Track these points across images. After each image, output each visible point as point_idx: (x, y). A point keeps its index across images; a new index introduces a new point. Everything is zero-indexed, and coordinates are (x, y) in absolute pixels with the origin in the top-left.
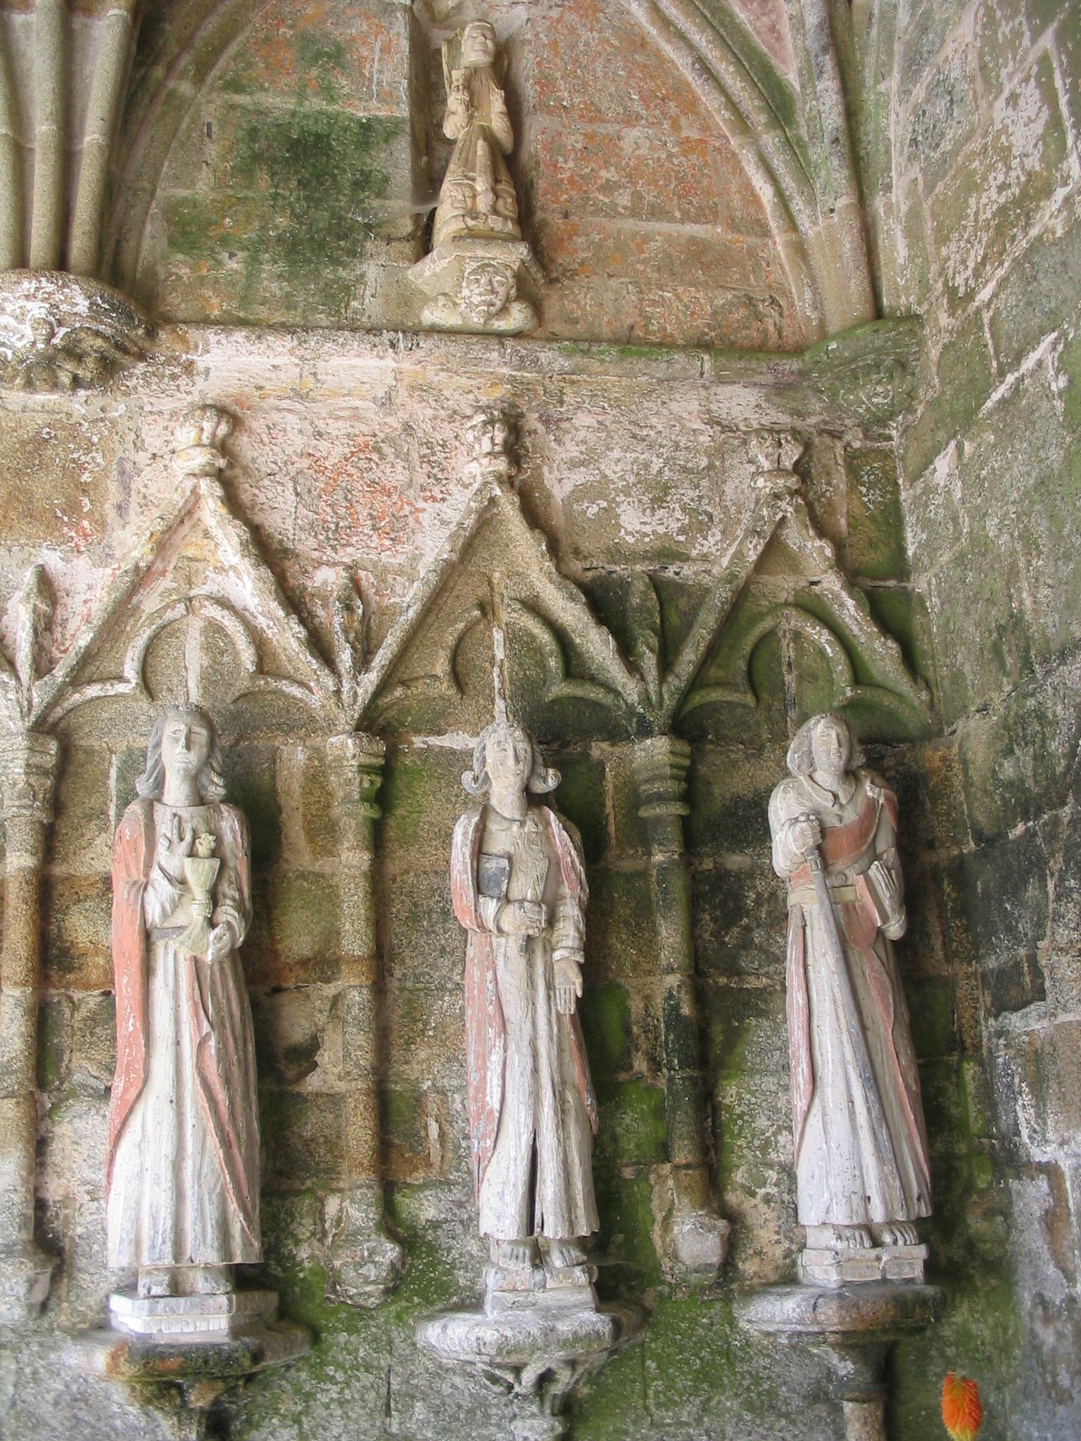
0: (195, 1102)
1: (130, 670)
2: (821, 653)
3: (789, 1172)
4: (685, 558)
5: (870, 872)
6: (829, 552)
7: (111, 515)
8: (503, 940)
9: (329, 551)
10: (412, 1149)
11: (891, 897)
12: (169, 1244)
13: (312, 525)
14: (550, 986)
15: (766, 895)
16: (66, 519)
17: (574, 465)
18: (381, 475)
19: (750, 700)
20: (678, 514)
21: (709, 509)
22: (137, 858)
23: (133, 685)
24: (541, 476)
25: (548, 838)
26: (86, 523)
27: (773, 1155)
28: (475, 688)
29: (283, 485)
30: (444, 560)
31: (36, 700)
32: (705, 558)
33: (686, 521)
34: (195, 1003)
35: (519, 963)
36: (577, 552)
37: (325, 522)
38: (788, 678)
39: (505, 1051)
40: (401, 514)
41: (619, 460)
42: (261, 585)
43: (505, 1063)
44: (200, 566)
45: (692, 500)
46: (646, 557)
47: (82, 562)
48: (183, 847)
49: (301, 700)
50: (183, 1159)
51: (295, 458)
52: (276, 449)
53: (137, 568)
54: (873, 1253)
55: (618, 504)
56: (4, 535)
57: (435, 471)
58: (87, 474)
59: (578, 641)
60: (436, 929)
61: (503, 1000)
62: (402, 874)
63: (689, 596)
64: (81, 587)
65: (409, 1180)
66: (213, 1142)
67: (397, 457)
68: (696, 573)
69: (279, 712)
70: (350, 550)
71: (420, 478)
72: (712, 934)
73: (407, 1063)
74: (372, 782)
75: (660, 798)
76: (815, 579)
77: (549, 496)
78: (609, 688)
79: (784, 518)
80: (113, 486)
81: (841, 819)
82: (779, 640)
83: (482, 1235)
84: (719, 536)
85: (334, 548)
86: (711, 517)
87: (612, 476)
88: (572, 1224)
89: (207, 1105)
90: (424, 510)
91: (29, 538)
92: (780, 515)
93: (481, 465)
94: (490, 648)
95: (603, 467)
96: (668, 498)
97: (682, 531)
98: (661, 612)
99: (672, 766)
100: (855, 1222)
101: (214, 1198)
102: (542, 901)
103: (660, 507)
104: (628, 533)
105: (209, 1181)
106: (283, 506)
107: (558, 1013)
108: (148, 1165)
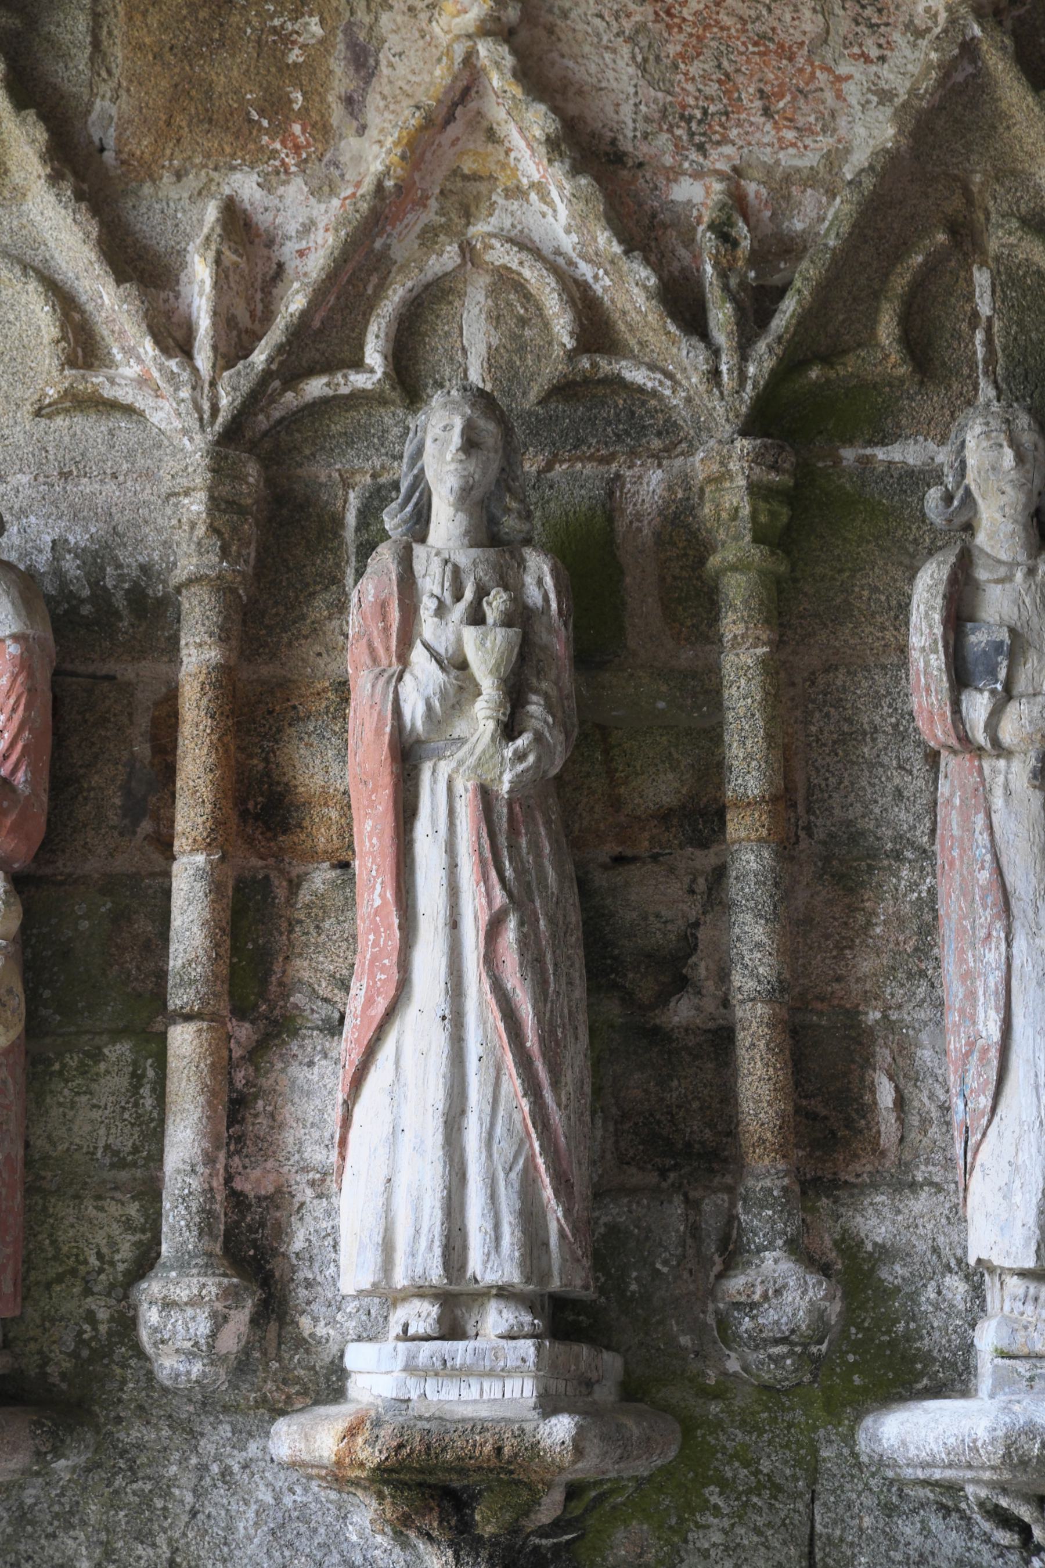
0: (483, 1021)
1: (374, 356)
7: (337, 114)
8: (1002, 763)
9: (694, 155)
10: (849, 1123)
12: (438, 1251)
13: (664, 112)
16: (265, 123)
18: (776, 24)
22: (386, 630)
23: (379, 374)
26: (297, 128)
28: (944, 364)
29: (614, 51)
30: (887, 151)
31: (224, 402)
34: (482, 862)
37: (684, 107)
39: (1009, 945)
40: (812, 87)
42: (581, 206)
44: (483, 187)
47: (295, 190)
48: (459, 610)
49: (654, 393)
50: (463, 1112)
53: (379, 187)
56: (168, 152)
58: (297, 51)
60: (885, 760)
61: (1004, 860)
62: (827, 671)
64: (292, 228)
65: (844, 1176)
66: (512, 1084)
69: (617, 415)
70: (728, 150)
71: (843, 26)
73: (839, 979)
74: (773, 514)
80: (338, 66)
83: (972, 1261)
85: (701, 148)
89: (501, 1026)
90: (850, 77)
91: (208, 155)
94: (970, 297)
101: (513, 1175)
105: (504, 1148)
106: (614, 85)
108: (406, 1122)
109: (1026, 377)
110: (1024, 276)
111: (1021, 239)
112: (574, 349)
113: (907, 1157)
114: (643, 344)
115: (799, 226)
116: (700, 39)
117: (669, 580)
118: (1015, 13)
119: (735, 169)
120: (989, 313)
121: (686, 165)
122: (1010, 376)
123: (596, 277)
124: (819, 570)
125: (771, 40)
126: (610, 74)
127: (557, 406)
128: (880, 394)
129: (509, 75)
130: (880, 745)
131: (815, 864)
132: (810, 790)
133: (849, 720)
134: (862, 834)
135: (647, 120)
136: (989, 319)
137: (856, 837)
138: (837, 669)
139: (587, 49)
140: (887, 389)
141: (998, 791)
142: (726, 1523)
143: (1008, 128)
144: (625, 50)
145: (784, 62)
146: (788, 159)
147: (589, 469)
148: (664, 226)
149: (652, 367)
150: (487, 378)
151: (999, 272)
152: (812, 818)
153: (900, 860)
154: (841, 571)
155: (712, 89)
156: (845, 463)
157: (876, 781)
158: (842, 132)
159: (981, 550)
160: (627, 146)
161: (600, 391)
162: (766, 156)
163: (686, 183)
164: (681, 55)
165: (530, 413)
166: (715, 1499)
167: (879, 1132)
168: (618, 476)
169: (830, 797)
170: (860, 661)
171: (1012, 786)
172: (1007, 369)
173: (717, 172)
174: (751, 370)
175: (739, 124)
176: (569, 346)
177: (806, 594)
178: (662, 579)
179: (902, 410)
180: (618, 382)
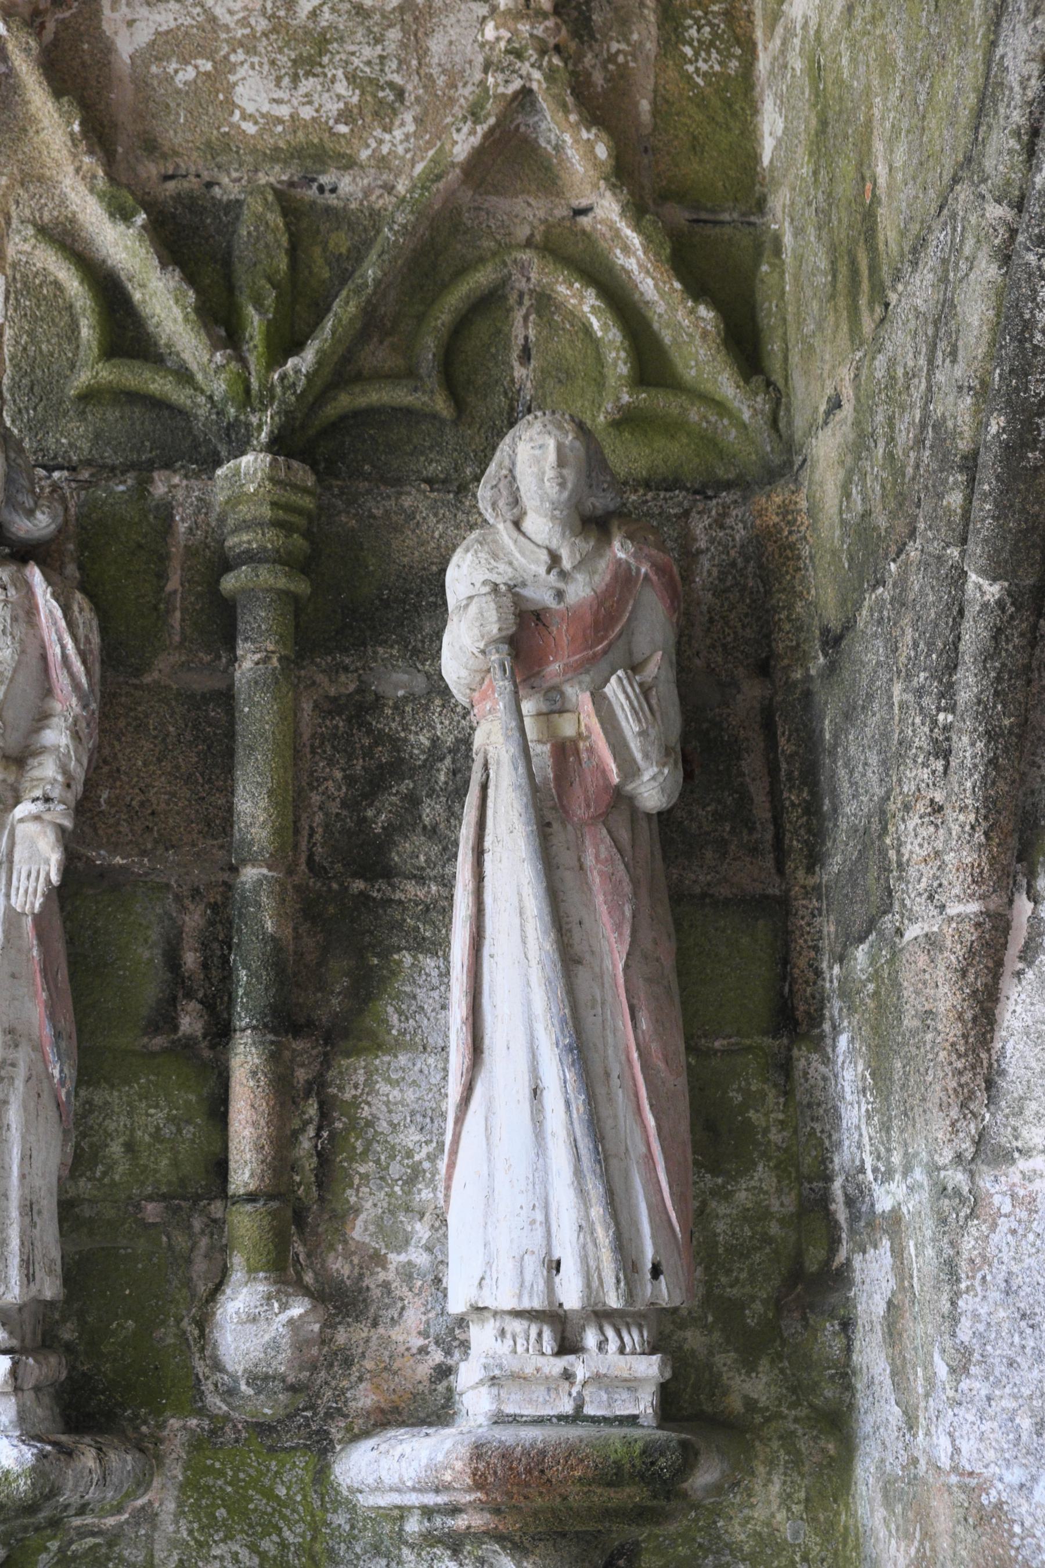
2: (587, 330)
3: (441, 1221)
4: (349, 163)
5: (608, 690)
6: (602, 151)
11: (643, 733)
15: (450, 740)
19: (441, 405)
20: (341, 87)
21: (397, 79)
32: (382, 162)
33: (355, 100)
36: (151, 146)
38: (519, 372)
45: (369, 63)
46: (275, 156)
54: (557, 1365)
55: (233, 69)
59: (137, 296)
63: (351, 228)
68: (367, 192)
72: (344, 804)
75: (250, 557)
76: (584, 203)
77: (108, 49)
78: (184, 376)
79: (526, 93)
81: (560, 595)
82: (510, 310)
84: (411, 128)
86: (400, 93)
87: (225, 18)
92: (517, 84)
96: (325, 60)
97: (346, 116)
98: (293, 251)
99: (274, 505)
100: (526, 1305)
103: (307, 74)
104: (244, 117)
109: (32, 389)
110: (41, 286)
111: (34, 247)
118: (60, 16)
143: (37, 132)
151: (14, 278)
172: (13, 379)
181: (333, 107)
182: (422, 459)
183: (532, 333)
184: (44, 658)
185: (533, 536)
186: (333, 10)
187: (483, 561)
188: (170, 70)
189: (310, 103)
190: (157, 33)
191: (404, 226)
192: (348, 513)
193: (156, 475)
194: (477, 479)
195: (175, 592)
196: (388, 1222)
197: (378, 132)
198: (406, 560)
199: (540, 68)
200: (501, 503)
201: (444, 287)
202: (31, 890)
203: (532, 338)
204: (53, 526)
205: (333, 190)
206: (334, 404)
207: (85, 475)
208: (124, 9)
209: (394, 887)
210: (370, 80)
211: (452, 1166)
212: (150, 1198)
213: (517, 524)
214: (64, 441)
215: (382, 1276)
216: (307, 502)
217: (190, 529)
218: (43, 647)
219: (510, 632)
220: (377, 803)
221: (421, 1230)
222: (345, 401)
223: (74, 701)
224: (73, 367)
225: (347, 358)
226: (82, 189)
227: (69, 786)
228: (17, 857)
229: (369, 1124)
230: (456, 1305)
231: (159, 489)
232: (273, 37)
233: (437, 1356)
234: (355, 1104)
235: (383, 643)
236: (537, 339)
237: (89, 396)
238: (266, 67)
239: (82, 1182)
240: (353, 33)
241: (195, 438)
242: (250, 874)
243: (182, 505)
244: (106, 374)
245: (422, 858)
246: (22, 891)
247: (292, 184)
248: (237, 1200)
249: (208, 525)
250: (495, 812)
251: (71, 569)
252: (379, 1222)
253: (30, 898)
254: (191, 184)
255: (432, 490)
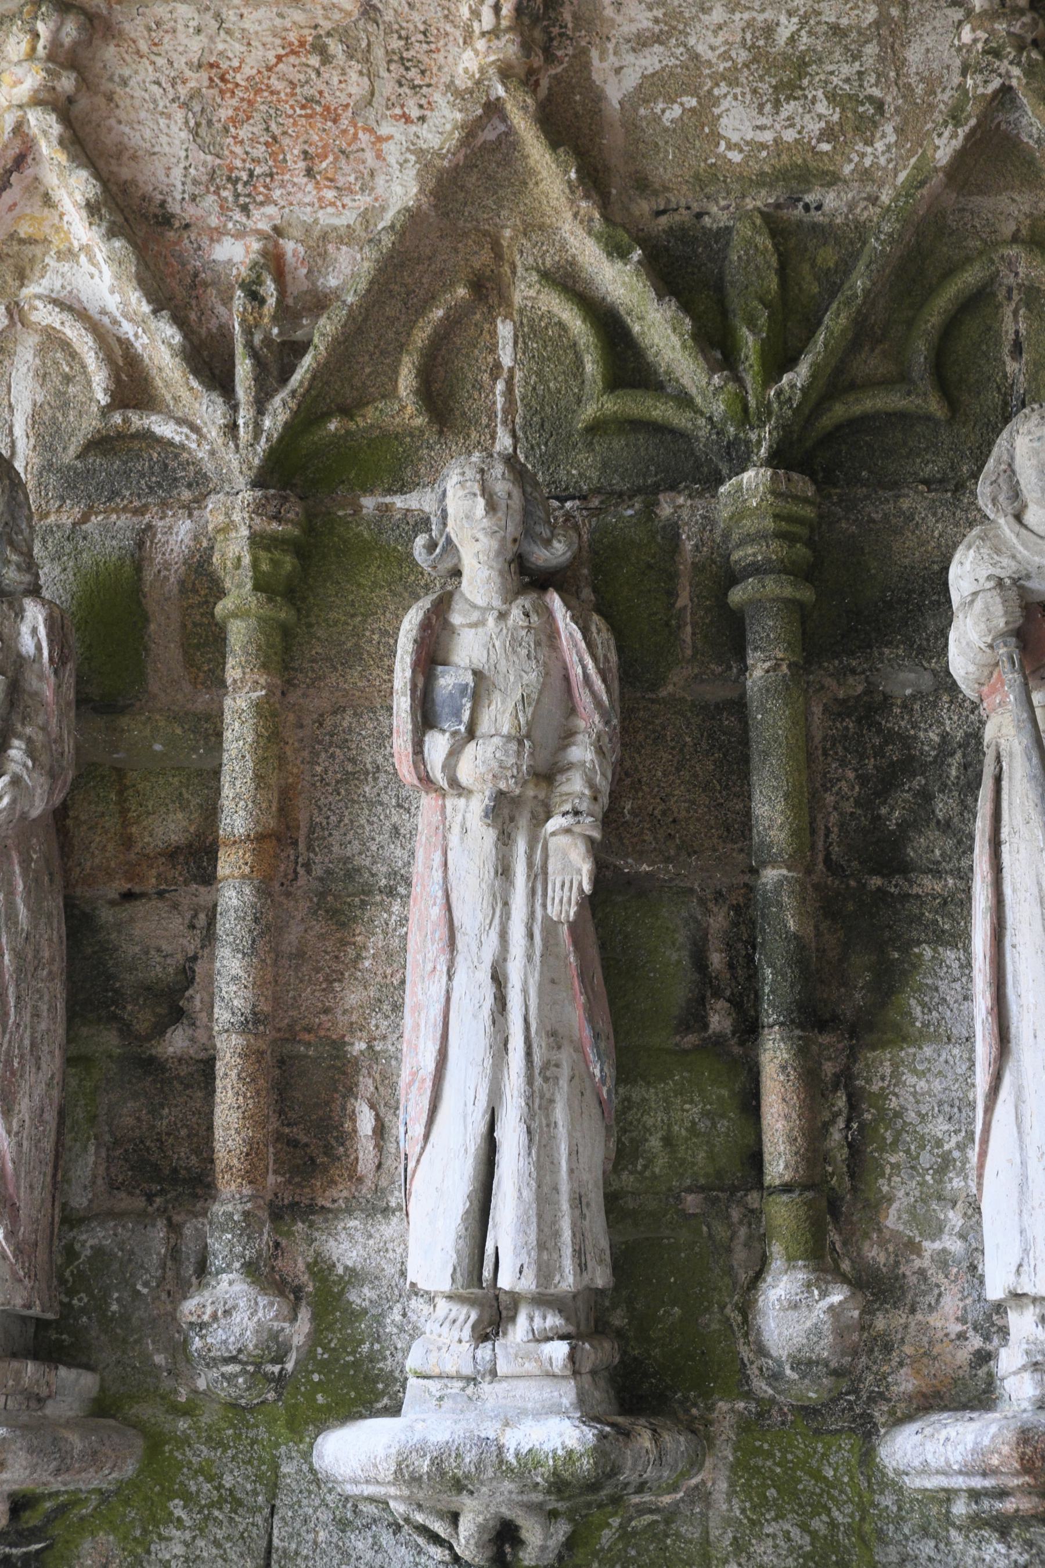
8: (462, 801)
9: (238, 216)
10: (328, 1150)
13: (212, 175)
14: (538, 876)
15: (959, 735)
17: (641, 42)
18: (323, 87)
19: (935, 406)
20: (822, 107)
21: (876, 92)
24: (587, 66)
25: (550, 636)
27: (957, 1183)
29: (169, 117)
32: (865, 175)
33: (836, 117)
35: (483, 837)
36: (642, 184)
38: (1011, 366)
39: (450, 978)
40: (354, 147)
41: (720, 27)
43: (448, 999)
44: (38, 250)
45: (847, 80)
46: (762, 180)
49: (183, 447)
51: (188, 73)
52: (161, 61)
57: (411, 74)
59: (636, 328)
60: (385, 798)
62: (335, 713)
63: (838, 242)
65: (321, 1202)
67: (351, 57)
68: (851, 206)
69: (151, 468)
70: (270, 210)
71: (387, 87)
72: (857, 803)
73: (326, 1011)
74: (275, 563)
75: (756, 570)
77: (597, 97)
78: (684, 400)
79: (1006, 90)
82: (1000, 305)
84: (892, 138)
85: (245, 209)
87: (708, 55)
88: (545, 1272)
90: (390, 137)
92: (996, 83)
93: (477, 53)
94: (493, 349)
95: (692, 41)
96: (805, 82)
97: (828, 134)
99: (776, 517)
102: (528, 736)
103: (788, 99)
104: (730, 147)
106: (167, 149)
107: (546, 918)
110: (546, 328)
111: (539, 292)
112: (108, 406)
113: (384, 1183)
114: (176, 399)
115: (333, 282)
116: (251, 103)
117: (189, 626)
118: (553, 72)
119: (275, 228)
120: (511, 364)
121: (230, 225)
122: (527, 424)
123: (136, 335)
124: (333, 615)
125: (318, 103)
126: (164, 139)
127: (95, 460)
128: (401, 444)
129: (55, 143)
130: (381, 785)
131: (311, 901)
132: (312, 830)
133: (353, 761)
134: (358, 870)
135: (195, 182)
136: (511, 370)
137: (351, 873)
138: (344, 711)
139: (143, 115)
140: (408, 439)
141: (456, 829)
142: (188, 1536)
143: (537, 183)
144: (179, 115)
145: (329, 124)
146: (327, 218)
147: (123, 521)
148: (205, 285)
149: (180, 421)
150: (31, 434)
151: (522, 323)
152: (312, 855)
153: (393, 896)
154: (353, 616)
155: (259, 151)
156: (365, 511)
157: (375, 819)
158: (379, 191)
159: (463, 595)
160: (174, 208)
161: (136, 445)
162: (306, 215)
163: (227, 241)
164: (232, 119)
165: (69, 468)
166: (179, 1512)
167: (357, 1159)
168: (150, 527)
169: (330, 835)
170: (367, 704)
171: (468, 825)
172: (524, 418)
173: (258, 232)
174: (267, 423)
175: (282, 186)
176: (103, 403)
177: (318, 639)
178: (184, 626)
179: (420, 459)
180: (148, 436)
181: (815, 127)
182: (918, 461)
183: (1022, 327)
184: (566, 678)
185: (1035, 529)
186: (810, 33)
187: (986, 557)
188: (658, 111)
189: (793, 125)
190: (644, 76)
191: (891, 235)
192: (848, 519)
193: (661, 497)
194: (975, 476)
195: (685, 607)
196: (921, 1210)
197: (860, 147)
198: (907, 561)
199: (1019, 64)
200: (1001, 498)
201: (931, 291)
202: (565, 899)
203: (1023, 332)
204: (569, 554)
205: (819, 208)
206: (829, 415)
207: (595, 502)
208: (612, 58)
209: (911, 883)
210: (850, 97)
211: (983, 1154)
212: (689, 1190)
213: (1018, 518)
214: (574, 472)
215: (917, 1263)
216: (808, 512)
217: (696, 546)
218: (566, 669)
219: (1017, 625)
220: (890, 801)
221: (955, 1218)
222: (839, 411)
223: (597, 718)
224: (579, 401)
225: (840, 370)
226: (581, 233)
227: (595, 799)
228: (551, 869)
229: (898, 1114)
230: (995, 1291)
231: (666, 510)
232: (754, 67)
233: (976, 1342)
234: (883, 1095)
235: (889, 644)
236: (1028, 333)
237: (595, 428)
238: (748, 96)
239: (625, 1175)
240: (831, 53)
241: (697, 459)
242: (771, 875)
243: (687, 524)
244: (611, 405)
245: (937, 852)
246: (557, 900)
247: (778, 206)
248: (774, 1190)
249: (714, 541)
250: (1010, 804)
251: (587, 593)
252: (912, 1210)
253: (565, 907)
254: (683, 216)
255: (929, 491)
